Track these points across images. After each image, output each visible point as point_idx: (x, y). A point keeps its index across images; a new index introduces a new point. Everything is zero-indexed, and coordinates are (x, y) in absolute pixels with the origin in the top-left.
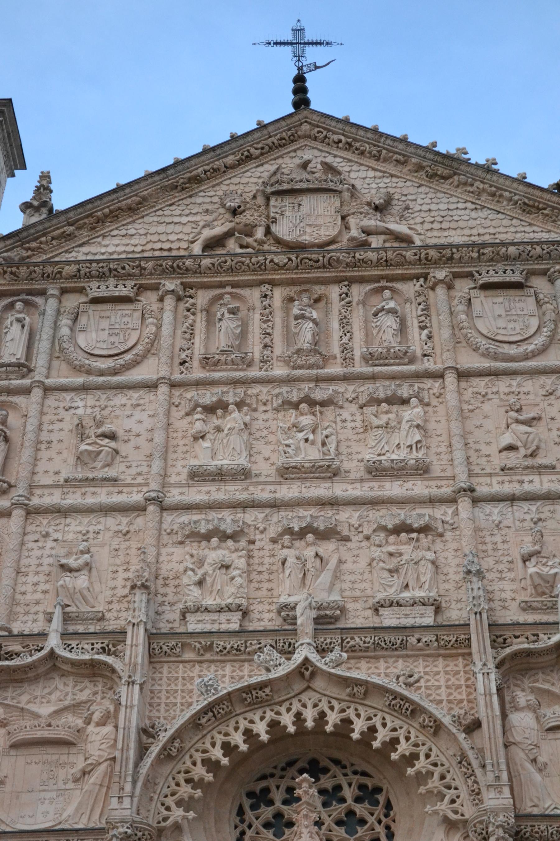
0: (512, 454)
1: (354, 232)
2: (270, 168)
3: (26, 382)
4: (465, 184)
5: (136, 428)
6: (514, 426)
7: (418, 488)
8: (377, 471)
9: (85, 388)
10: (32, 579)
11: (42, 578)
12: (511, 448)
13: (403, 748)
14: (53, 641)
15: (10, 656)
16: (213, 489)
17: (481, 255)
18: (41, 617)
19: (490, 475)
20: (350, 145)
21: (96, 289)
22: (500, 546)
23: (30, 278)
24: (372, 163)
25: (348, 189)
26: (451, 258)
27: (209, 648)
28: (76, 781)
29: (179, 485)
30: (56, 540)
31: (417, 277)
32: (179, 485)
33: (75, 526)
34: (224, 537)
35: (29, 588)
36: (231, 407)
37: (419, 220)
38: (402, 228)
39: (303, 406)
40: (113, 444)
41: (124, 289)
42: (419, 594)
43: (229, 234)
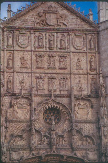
0: (78, 67)
1: (59, 24)
6: (79, 62)
7: (66, 72)
9: (21, 51)
11: (19, 83)
12: (78, 66)
15: (17, 96)
17: (76, 30)
18: (19, 89)
28: (26, 113)
29: (35, 69)
30: (20, 77)
31: (67, 33)
34: (42, 78)
35: (17, 85)
36: (42, 57)
38: (66, 23)
39: (51, 57)
40: (26, 62)
42: (65, 89)
43: (41, 21)
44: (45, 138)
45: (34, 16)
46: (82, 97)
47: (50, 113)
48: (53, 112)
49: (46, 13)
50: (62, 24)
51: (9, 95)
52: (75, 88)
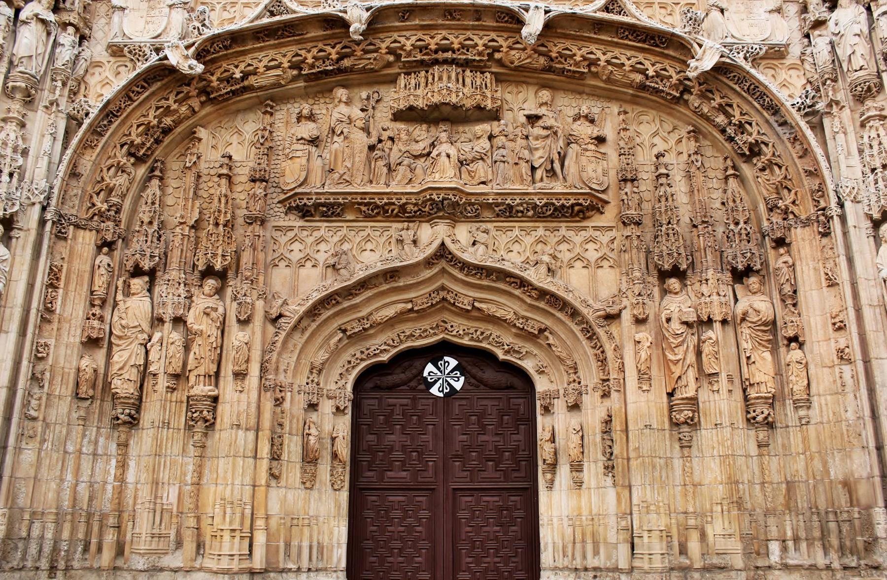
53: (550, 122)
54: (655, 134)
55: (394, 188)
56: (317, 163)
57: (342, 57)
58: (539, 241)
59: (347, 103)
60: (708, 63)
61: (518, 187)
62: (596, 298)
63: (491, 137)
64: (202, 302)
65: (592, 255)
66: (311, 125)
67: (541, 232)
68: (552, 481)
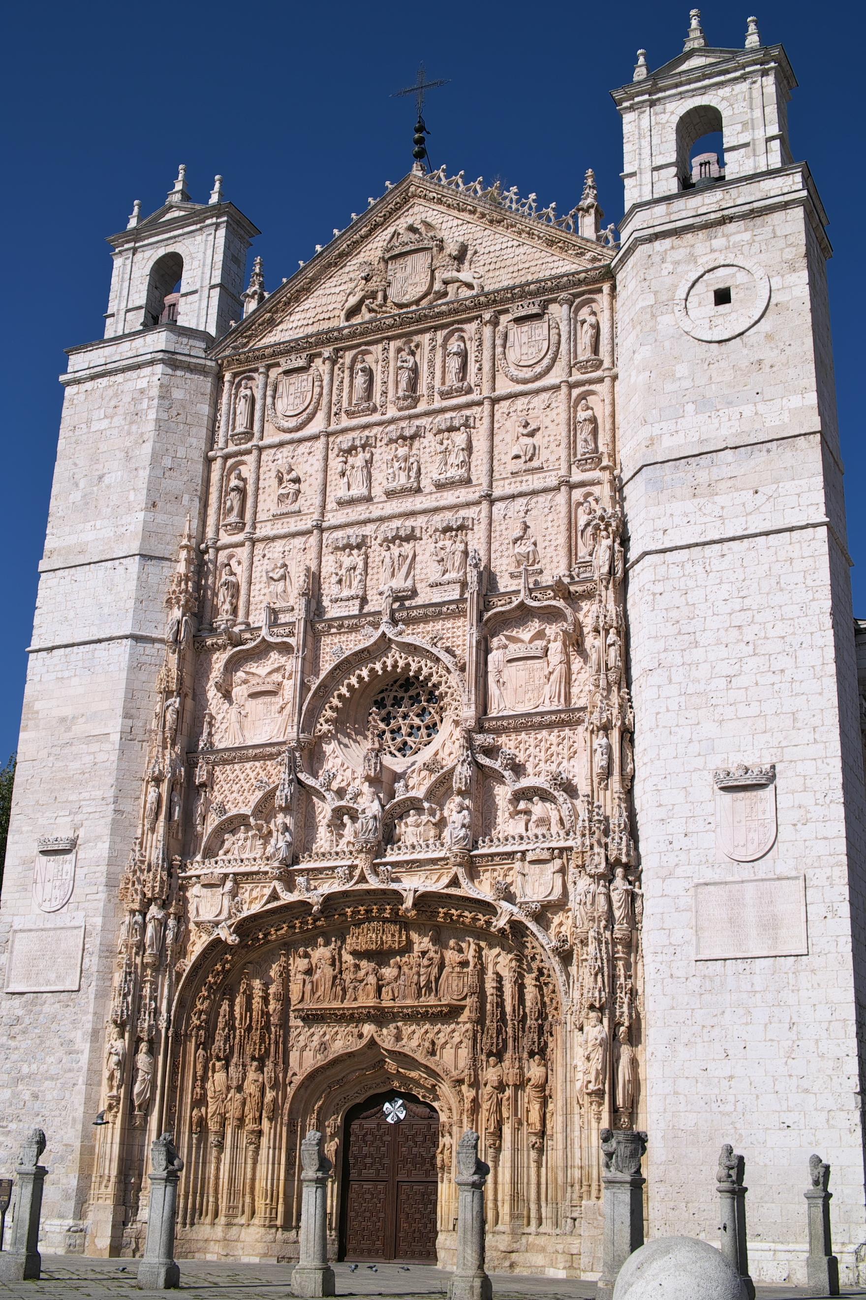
1: (438, 286)
2: (391, 230)
3: (249, 445)
4: (512, 226)
5: (311, 471)
8: (440, 486)
9: (281, 445)
10: (258, 587)
11: (263, 585)
12: (517, 457)
13: (435, 679)
14: (264, 632)
16: (350, 510)
19: (504, 479)
20: (439, 199)
21: (286, 364)
22: (504, 532)
23: (248, 360)
24: (455, 213)
25: (437, 245)
26: (495, 301)
27: (342, 626)
29: (332, 511)
31: (476, 318)
32: (332, 511)
33: (279, 545)
34: (351, 548)
37: (482, 263)
41: (301, 363)
43: (361, 302)
44: (346, 818)
45: (342, 288)
46: (522, 604)
47: (397, 702)
48: (411, 698)
49: (386, 262)
50: (457, 284)
51: (216, 644)
52: (503, 566)
53: (431, 954)
54: (499, 955)
55: (346, 1005)
56: (308, 987)
57: (315, 921)
58: (426, 1032)
59: (325, 946)
60: (501, 922)
61: (409, 1002)
62: (456, 1068)
63: (400, 968)
64: (252, 1075)
65: (457, 1039)
66: (307, 960)
67: (426, 1027)
68: (442, 1178)
